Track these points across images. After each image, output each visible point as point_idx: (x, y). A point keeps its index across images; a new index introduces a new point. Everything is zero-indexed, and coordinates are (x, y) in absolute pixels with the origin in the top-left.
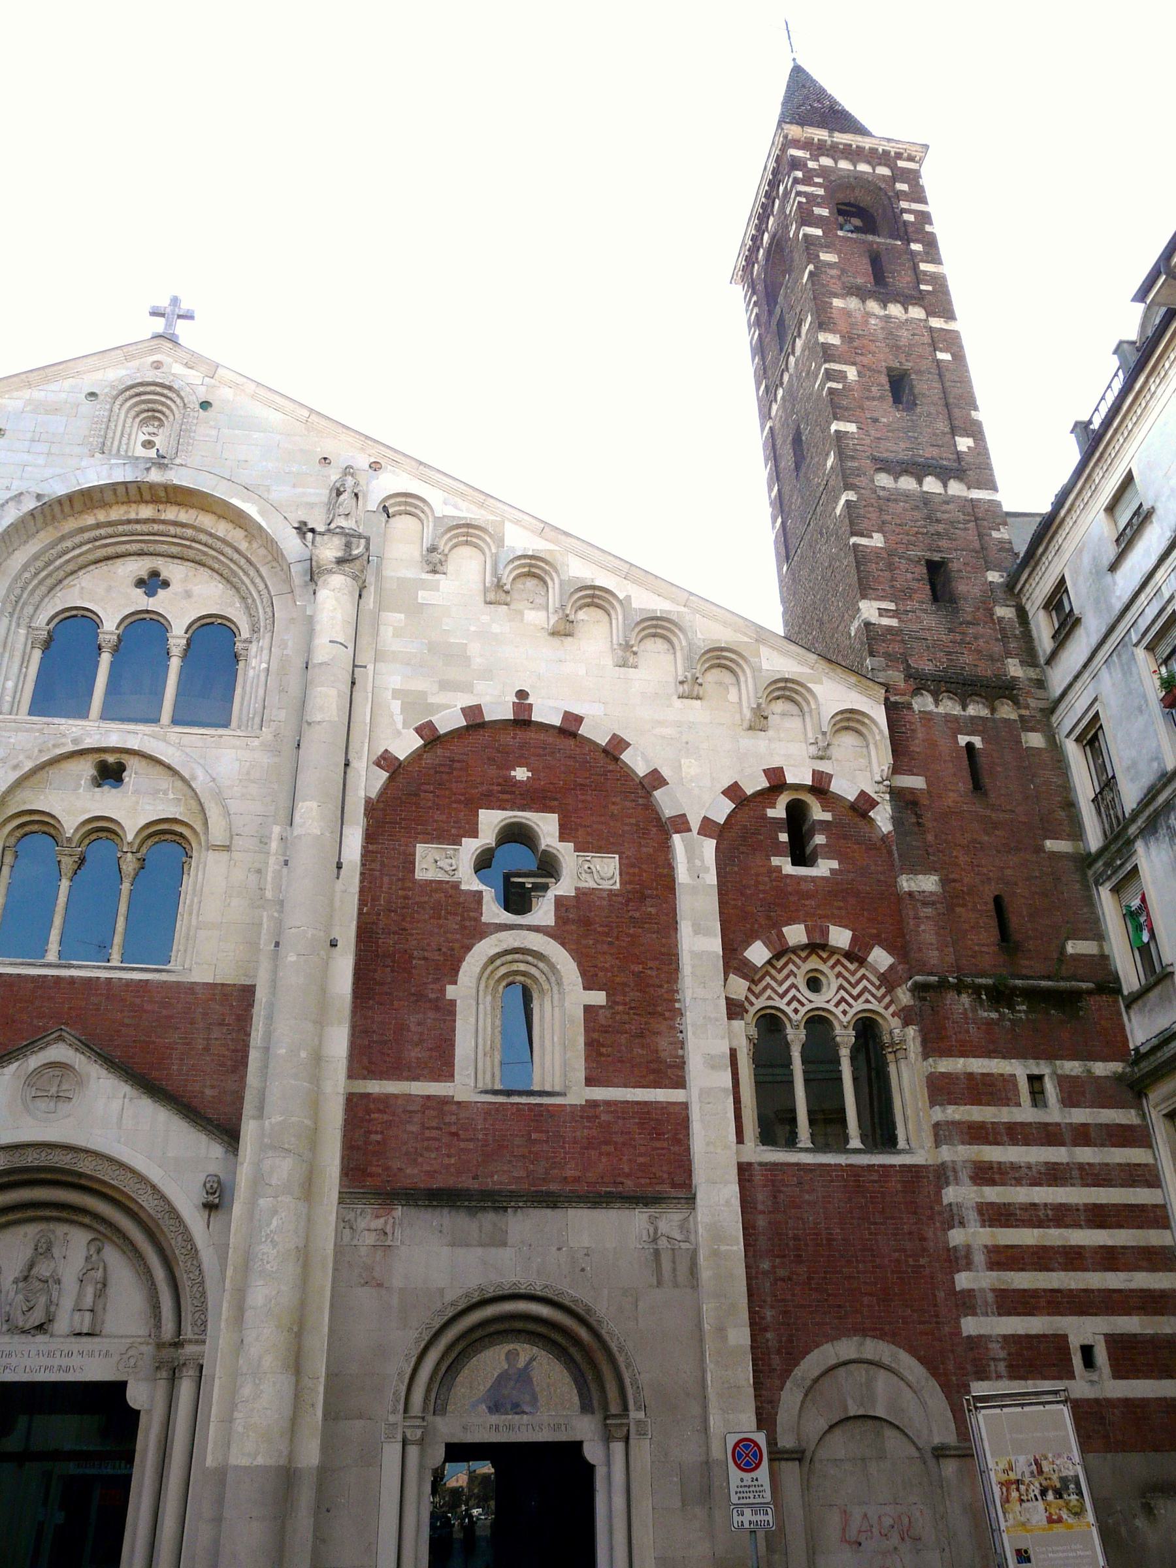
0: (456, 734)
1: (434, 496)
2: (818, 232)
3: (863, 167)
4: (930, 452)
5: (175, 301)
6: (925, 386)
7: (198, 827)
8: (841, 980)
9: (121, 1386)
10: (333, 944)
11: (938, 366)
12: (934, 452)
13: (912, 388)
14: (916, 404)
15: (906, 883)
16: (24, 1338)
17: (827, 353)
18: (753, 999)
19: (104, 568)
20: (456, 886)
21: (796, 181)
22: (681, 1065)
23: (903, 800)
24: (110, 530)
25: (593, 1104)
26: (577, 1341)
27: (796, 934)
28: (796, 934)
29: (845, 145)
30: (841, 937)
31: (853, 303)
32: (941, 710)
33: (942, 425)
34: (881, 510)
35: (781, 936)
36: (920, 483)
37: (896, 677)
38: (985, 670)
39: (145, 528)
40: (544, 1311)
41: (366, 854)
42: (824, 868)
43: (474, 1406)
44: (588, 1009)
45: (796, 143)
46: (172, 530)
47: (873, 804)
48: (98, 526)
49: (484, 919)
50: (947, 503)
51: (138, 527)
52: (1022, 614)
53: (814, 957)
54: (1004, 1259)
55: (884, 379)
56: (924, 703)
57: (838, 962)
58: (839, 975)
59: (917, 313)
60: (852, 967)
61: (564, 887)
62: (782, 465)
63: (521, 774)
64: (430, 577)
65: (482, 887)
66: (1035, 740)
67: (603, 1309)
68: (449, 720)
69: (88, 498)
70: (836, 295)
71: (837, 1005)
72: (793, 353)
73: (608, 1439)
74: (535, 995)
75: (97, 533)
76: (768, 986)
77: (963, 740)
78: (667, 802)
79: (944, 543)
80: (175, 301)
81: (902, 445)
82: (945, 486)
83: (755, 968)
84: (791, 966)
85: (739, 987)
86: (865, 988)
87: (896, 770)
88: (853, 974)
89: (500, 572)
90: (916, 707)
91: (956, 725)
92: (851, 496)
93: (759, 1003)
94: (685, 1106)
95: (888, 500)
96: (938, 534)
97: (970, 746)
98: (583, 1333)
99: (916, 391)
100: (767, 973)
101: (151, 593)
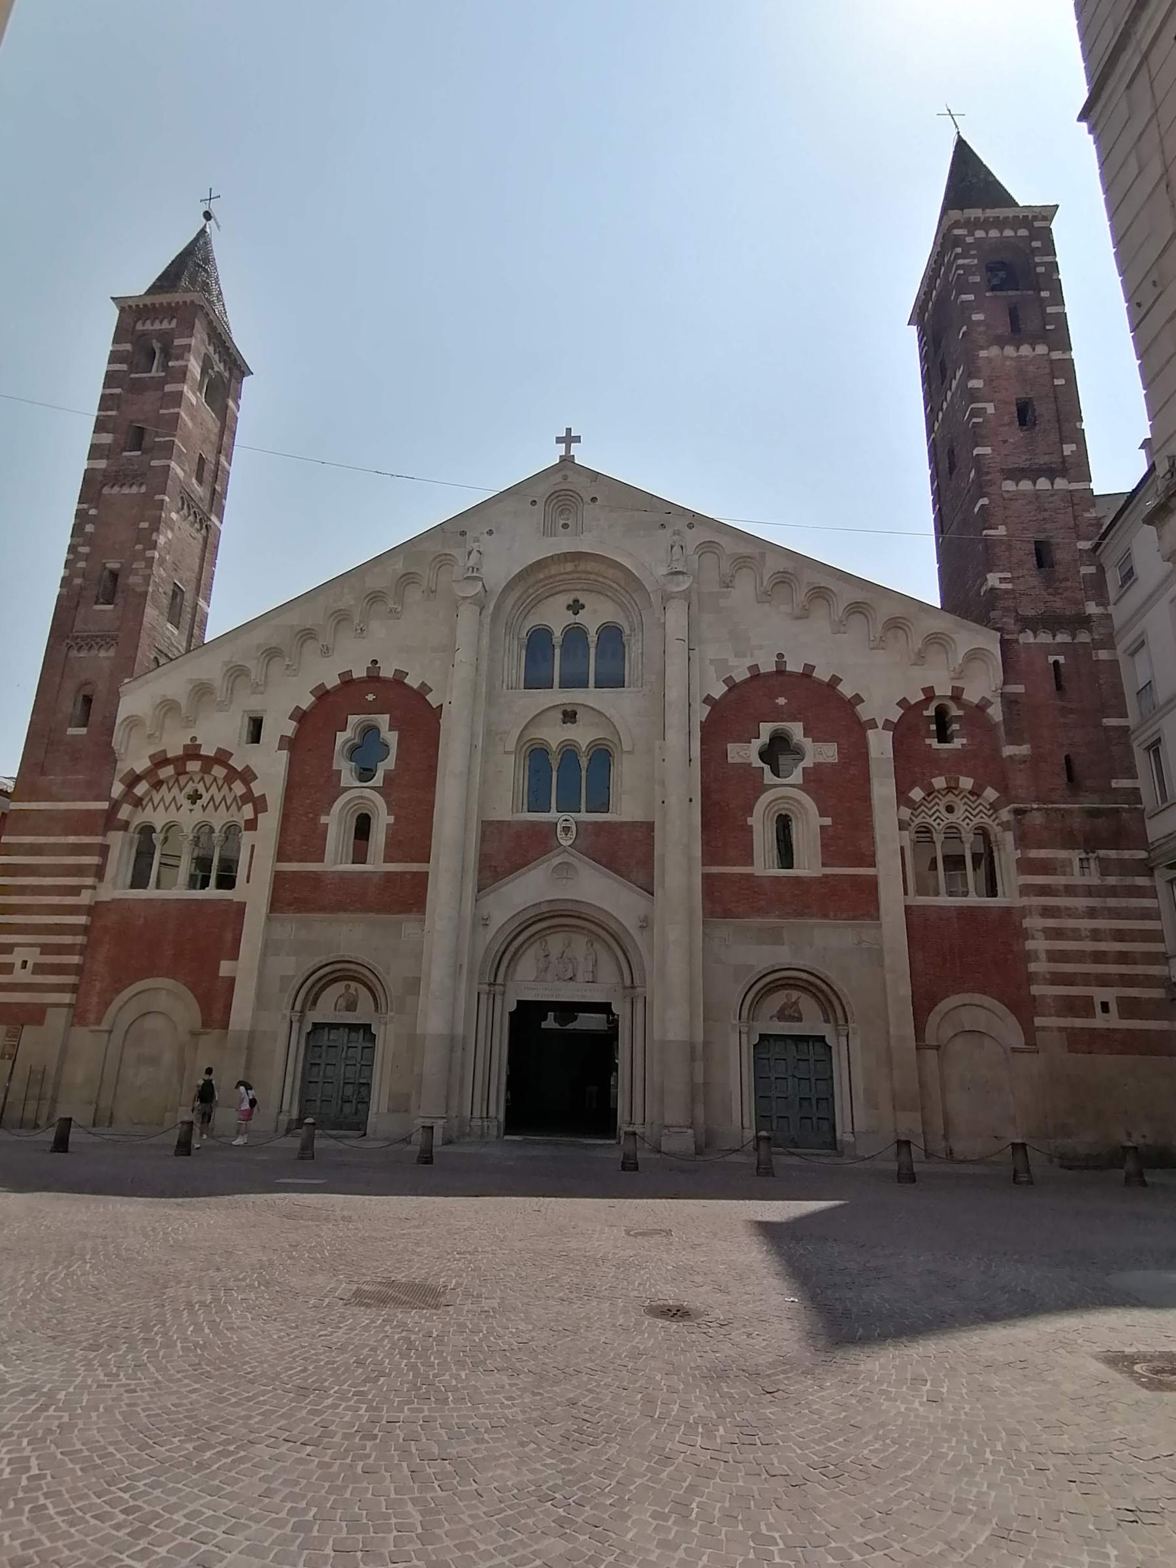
0: (745, 682)
1: (723, 540)
2: (971, 297)
3: (1008, 233)
4: (1042, 460)
5: (569, 430)
6: (1044, 410)
7: (617, 742)
8: (966, 807)
9: (610, 1004)
10: (691, 800)
11: (1055, 391)
12: (1047, 458)
13: (1034, 410)
14: (1035, 425)
15: (1008, 750)
16: (565, 983)
17: (973, 395)
18: (913, 818)
19: (551, 599)
20: (750, 764)
21: (957, 257)
22: (874, 855)
23: (1009, 702)
24: (551, 580)
25: (826, 876)
26: (822, 991)
27: (939, 782)
28: (939, 782)
29: (994, 217)
30: (966, 783)
31: (994, 351)
32: (1037, 641)
33: (1054, 437)
34: (1005, 508)
35: (931, 784)
36: (1035, 484)
37: (1010, 622)
38: (1070, 611)
39: (569, 577)
40: (804, 976)
41: (703, 751)
42: (958, 743)
43: (771, 1018)
44: (822, 827)
45: (956, 224)
46: (584, 576)
47: (991, 704)
48: (546, 578)
49: (765, 782)
50: (1052, 495)
51: (566, 576)
52: (1101, 569)
53: (950, 794)
54: (1054, 956)
55: (1014, 409)
56: (1028, 638)
57: (965, 796)
58: (965, 803)
59: (1041, 349)
60: (973, 799)
61: (808, 762)
62: (941, 467)
63: (781, 701)
64: (725, 590)
65: (763, 765)
66: (1103, 655)
67: (833, 976)
68: (741, 675)
69: (540, 564)
70: (982, 348)
71: (963, 820)
72: (950, 389)
73: (838, 1035)
74: (793, 819)
75: (546, 582)
76: (923, 811)
77: (1051, 659)
78: (864, 712)
79: (1047, 526)
80: (569, 430)
81: (1024, 457)
82: (1052, 484)
83: (914, 801)
84: (937, 800)
85: (906, 813)
86: (981, 811)
87: (1005, 683)
88: (973, 802)
89: (765, 584)
90: (1021, 641)
91: (1047, 649)
92: (984, 501)
93: (917, 821)
94: (876, 876)
95: (1011, 500)
96: (1044, 519)
97: (1056, 663)
98: (824, 987)
99: (1036, 414)
100: (922, 804)
101: (576, 613)
